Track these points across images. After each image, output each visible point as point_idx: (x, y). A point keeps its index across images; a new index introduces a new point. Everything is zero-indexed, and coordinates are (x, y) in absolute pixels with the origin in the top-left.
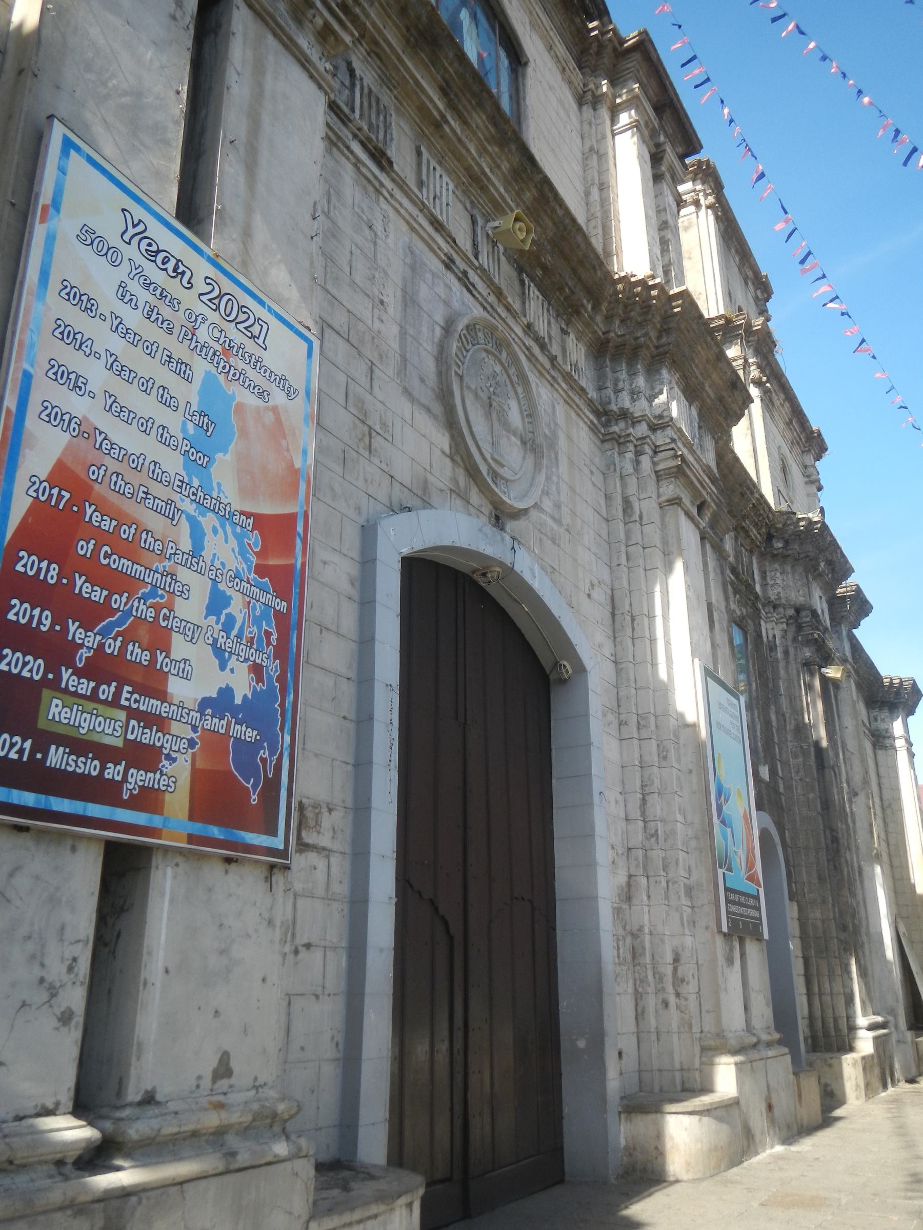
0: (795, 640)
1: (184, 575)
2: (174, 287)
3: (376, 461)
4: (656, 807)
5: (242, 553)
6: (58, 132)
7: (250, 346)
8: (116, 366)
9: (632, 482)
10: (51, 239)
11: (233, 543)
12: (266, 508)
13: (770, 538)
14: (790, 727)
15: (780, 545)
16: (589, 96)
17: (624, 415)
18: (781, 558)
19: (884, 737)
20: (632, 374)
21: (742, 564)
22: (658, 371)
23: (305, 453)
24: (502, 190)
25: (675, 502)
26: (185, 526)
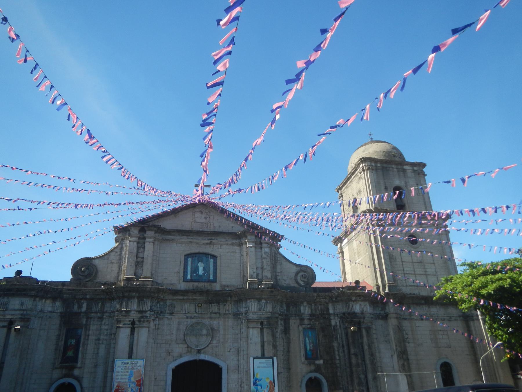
0: (343, 322)
1: (128, 389)
2: (127, 365)
3: (171, 356)
4: (242, 385)
5: (135, 385)
6: (115, 360)
7: (136, 365)
8: (121, 375)
9: (241, 326)
10: (115, 369)
11: (134, 384)
12: (137, 379)
13: (332, 299)
14: (341, 345)
15: (335, 299)
16: (241, 244)
17: (240, 313)
18: (337, 301)
19: (473, 317)
20: (243, 304)
21: (319, 310)
22: (247, 301)
23: (143, 372)
24: (199, 298)
25: (249, 327)
26: (128, 385)
